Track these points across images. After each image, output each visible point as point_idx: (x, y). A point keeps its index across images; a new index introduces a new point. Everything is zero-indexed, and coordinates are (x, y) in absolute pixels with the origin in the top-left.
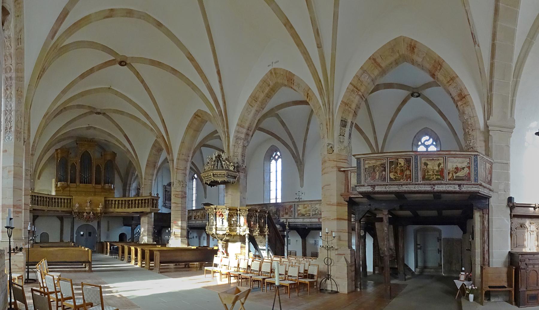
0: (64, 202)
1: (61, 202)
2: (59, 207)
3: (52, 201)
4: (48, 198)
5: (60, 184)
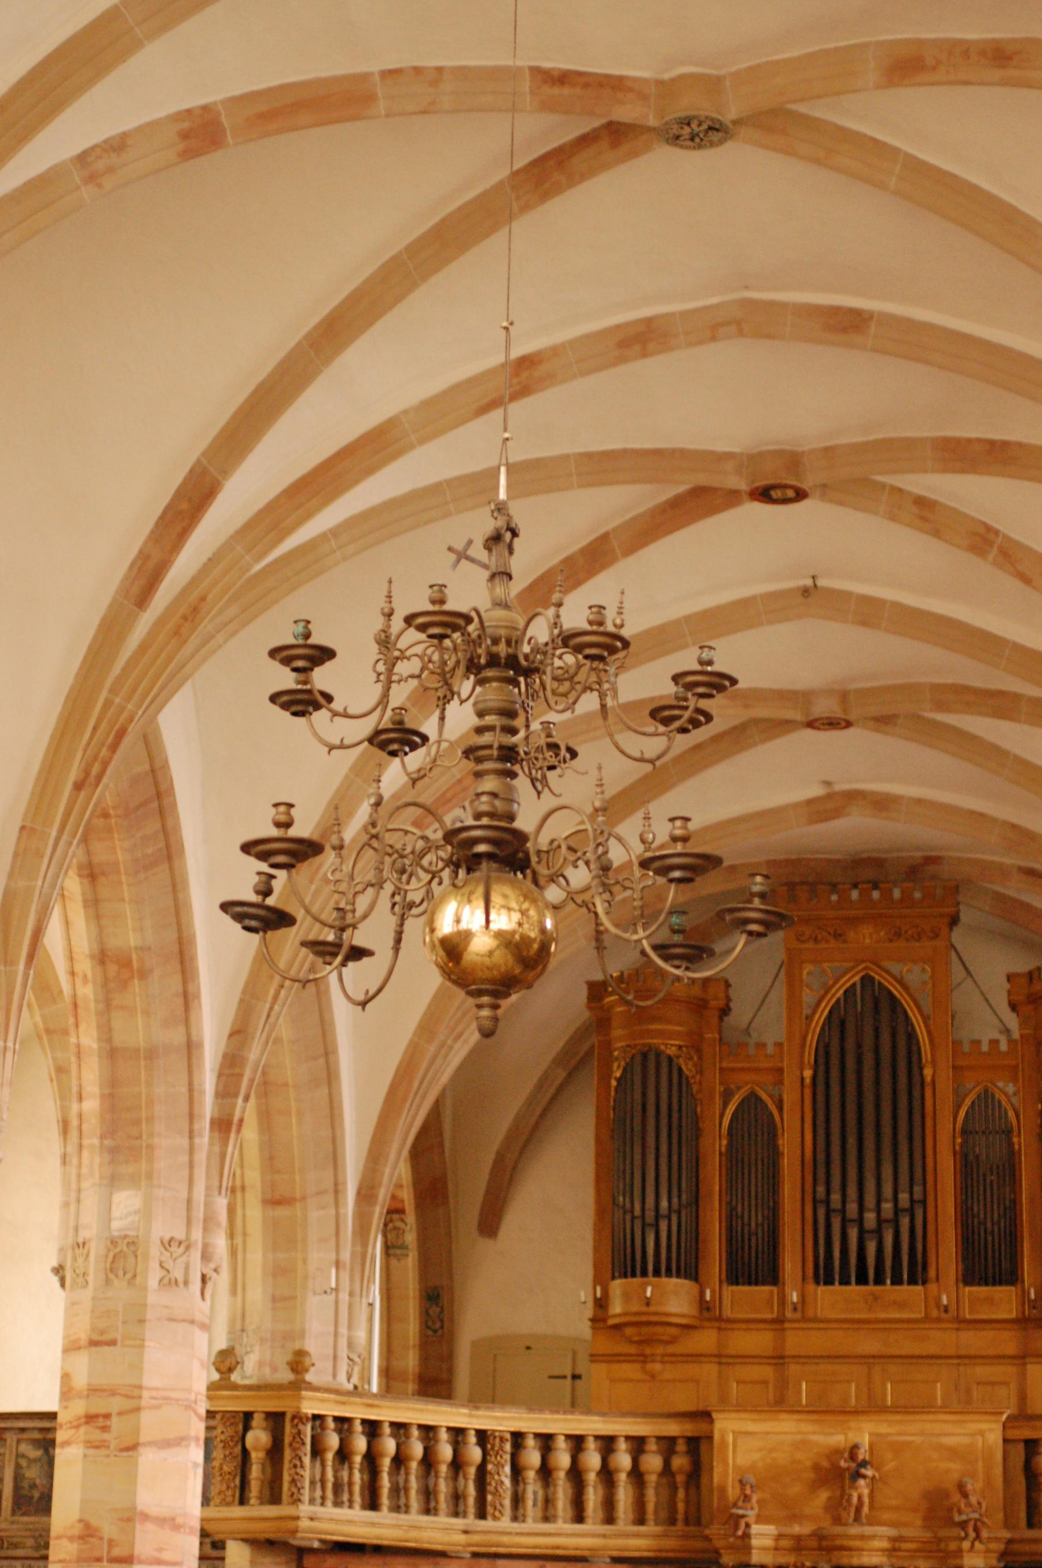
1: (607, 1474)
3: (517, 1472)
5: (626, 1297)
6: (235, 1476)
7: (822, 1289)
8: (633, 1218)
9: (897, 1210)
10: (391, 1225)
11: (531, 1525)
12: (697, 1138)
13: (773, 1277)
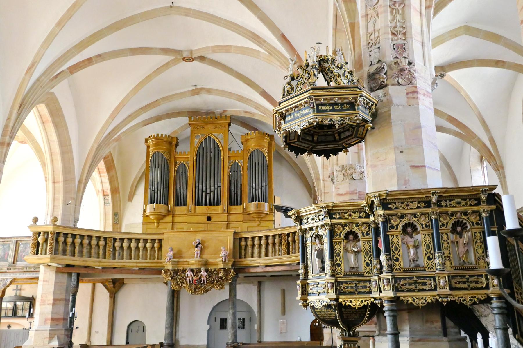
0: (145, 247)
1: (137, 248)
2: (132, 260)
4: (102, 239)
5: (150, 209)
6: (35, 248)
7: (197, 206)
8: (152, 190)
9: (214, 189)
10: (105, 199)
11: (116, 260)
12: (169, 173)
13: (185, 205)
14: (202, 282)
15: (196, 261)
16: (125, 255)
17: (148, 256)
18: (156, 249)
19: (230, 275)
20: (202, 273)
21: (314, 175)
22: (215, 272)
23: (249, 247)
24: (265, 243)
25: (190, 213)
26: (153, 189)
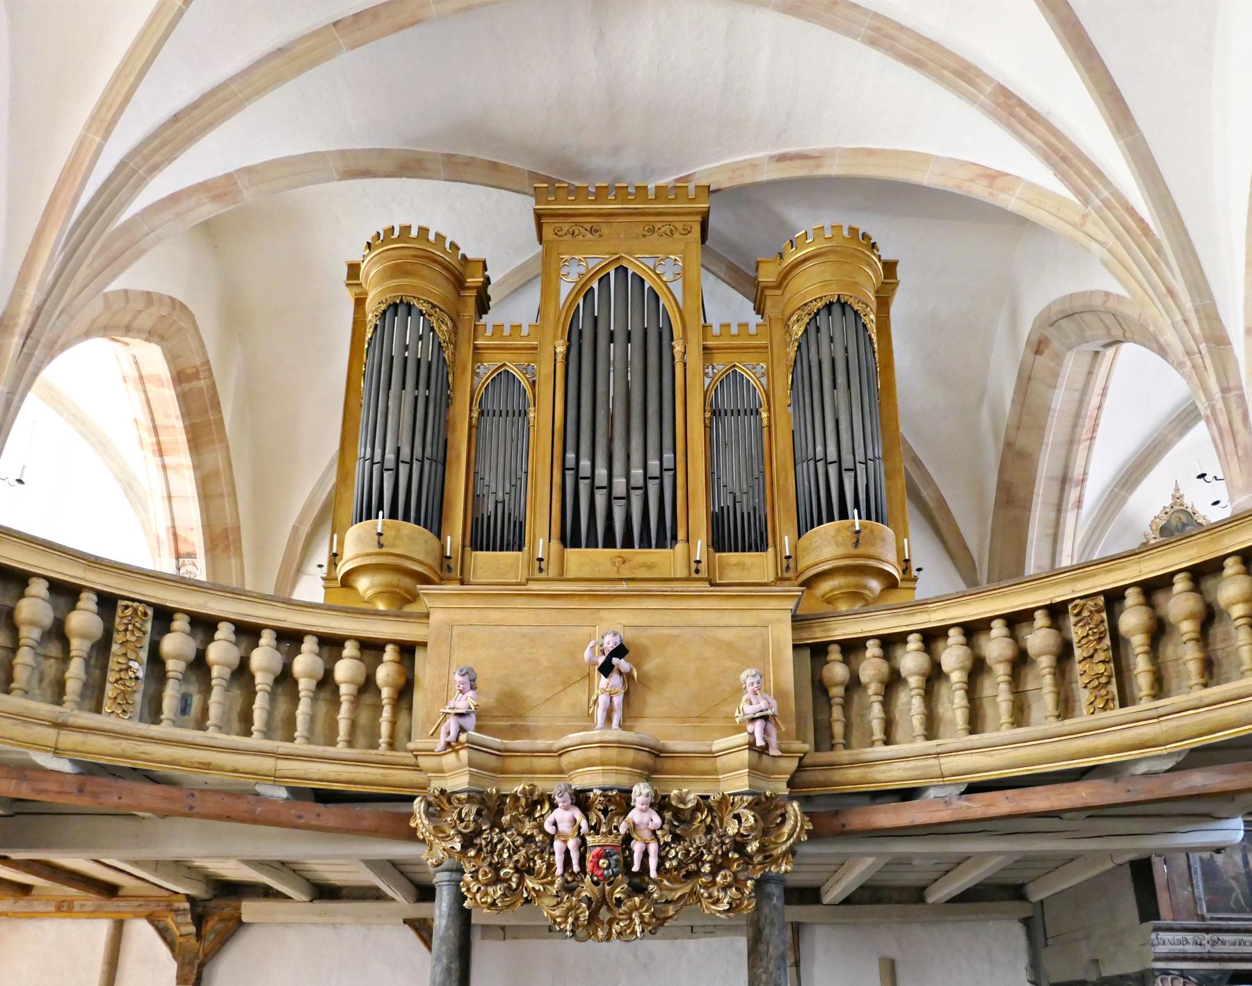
5: (360, 540)
7: (569, 551)
8: (373, 464)
9: (646, 477)
14: (636, 868)
15: (604, 745)
16: (214, 711)
17: (343, 726)
18: (386, 693)
19: (786, 829)
20: (634, 815)
21: (1199, 319)
22: (700, 817)
23: (873, 688)
24: (968, 664)
25: (537, 575)
26: (377, 458)
